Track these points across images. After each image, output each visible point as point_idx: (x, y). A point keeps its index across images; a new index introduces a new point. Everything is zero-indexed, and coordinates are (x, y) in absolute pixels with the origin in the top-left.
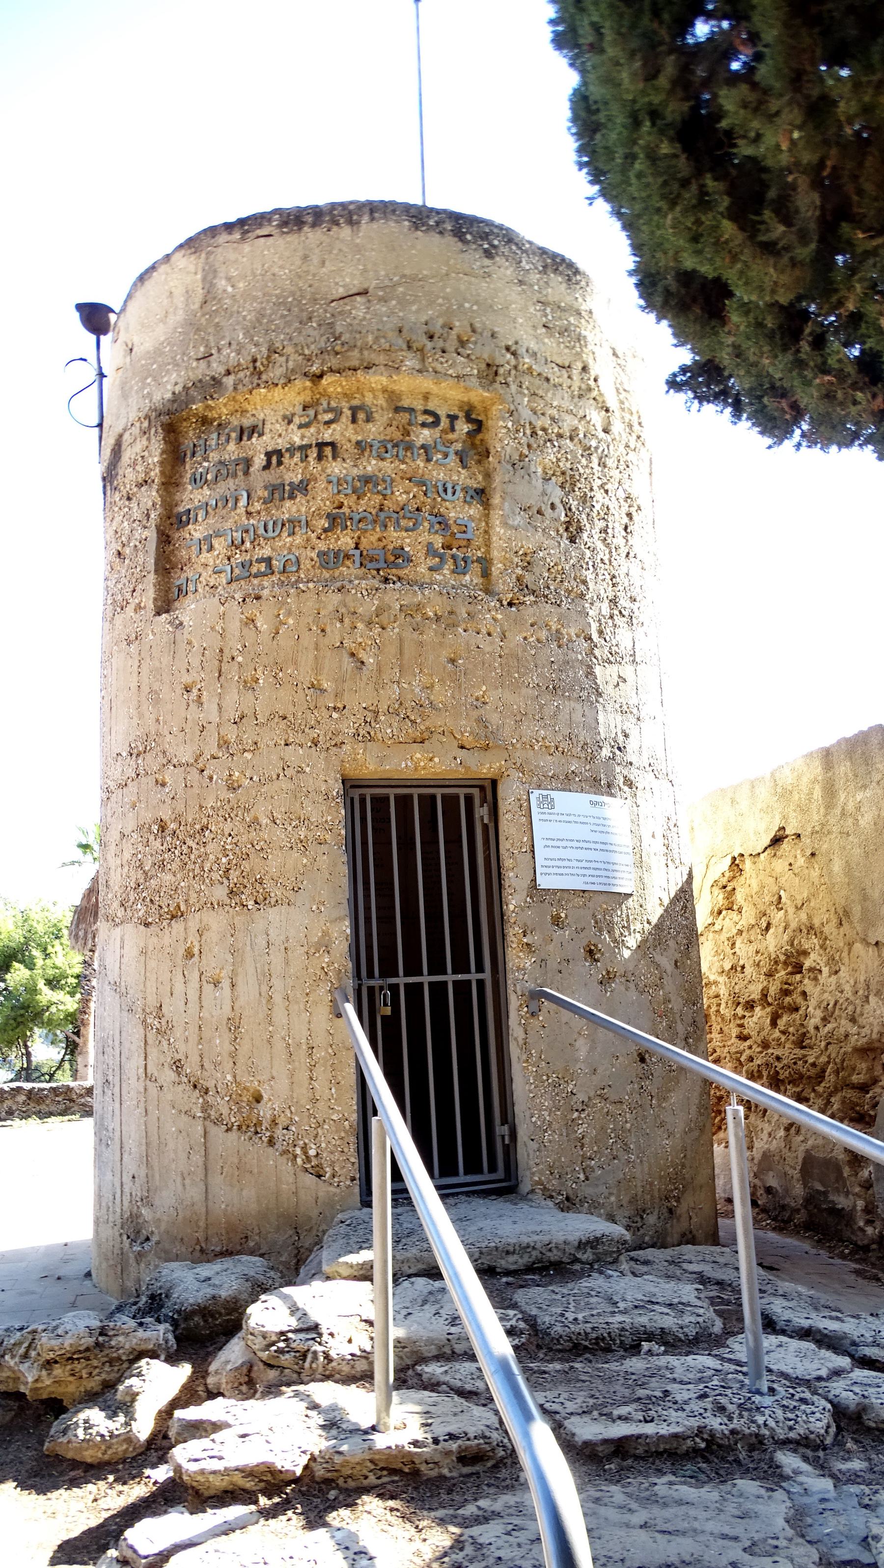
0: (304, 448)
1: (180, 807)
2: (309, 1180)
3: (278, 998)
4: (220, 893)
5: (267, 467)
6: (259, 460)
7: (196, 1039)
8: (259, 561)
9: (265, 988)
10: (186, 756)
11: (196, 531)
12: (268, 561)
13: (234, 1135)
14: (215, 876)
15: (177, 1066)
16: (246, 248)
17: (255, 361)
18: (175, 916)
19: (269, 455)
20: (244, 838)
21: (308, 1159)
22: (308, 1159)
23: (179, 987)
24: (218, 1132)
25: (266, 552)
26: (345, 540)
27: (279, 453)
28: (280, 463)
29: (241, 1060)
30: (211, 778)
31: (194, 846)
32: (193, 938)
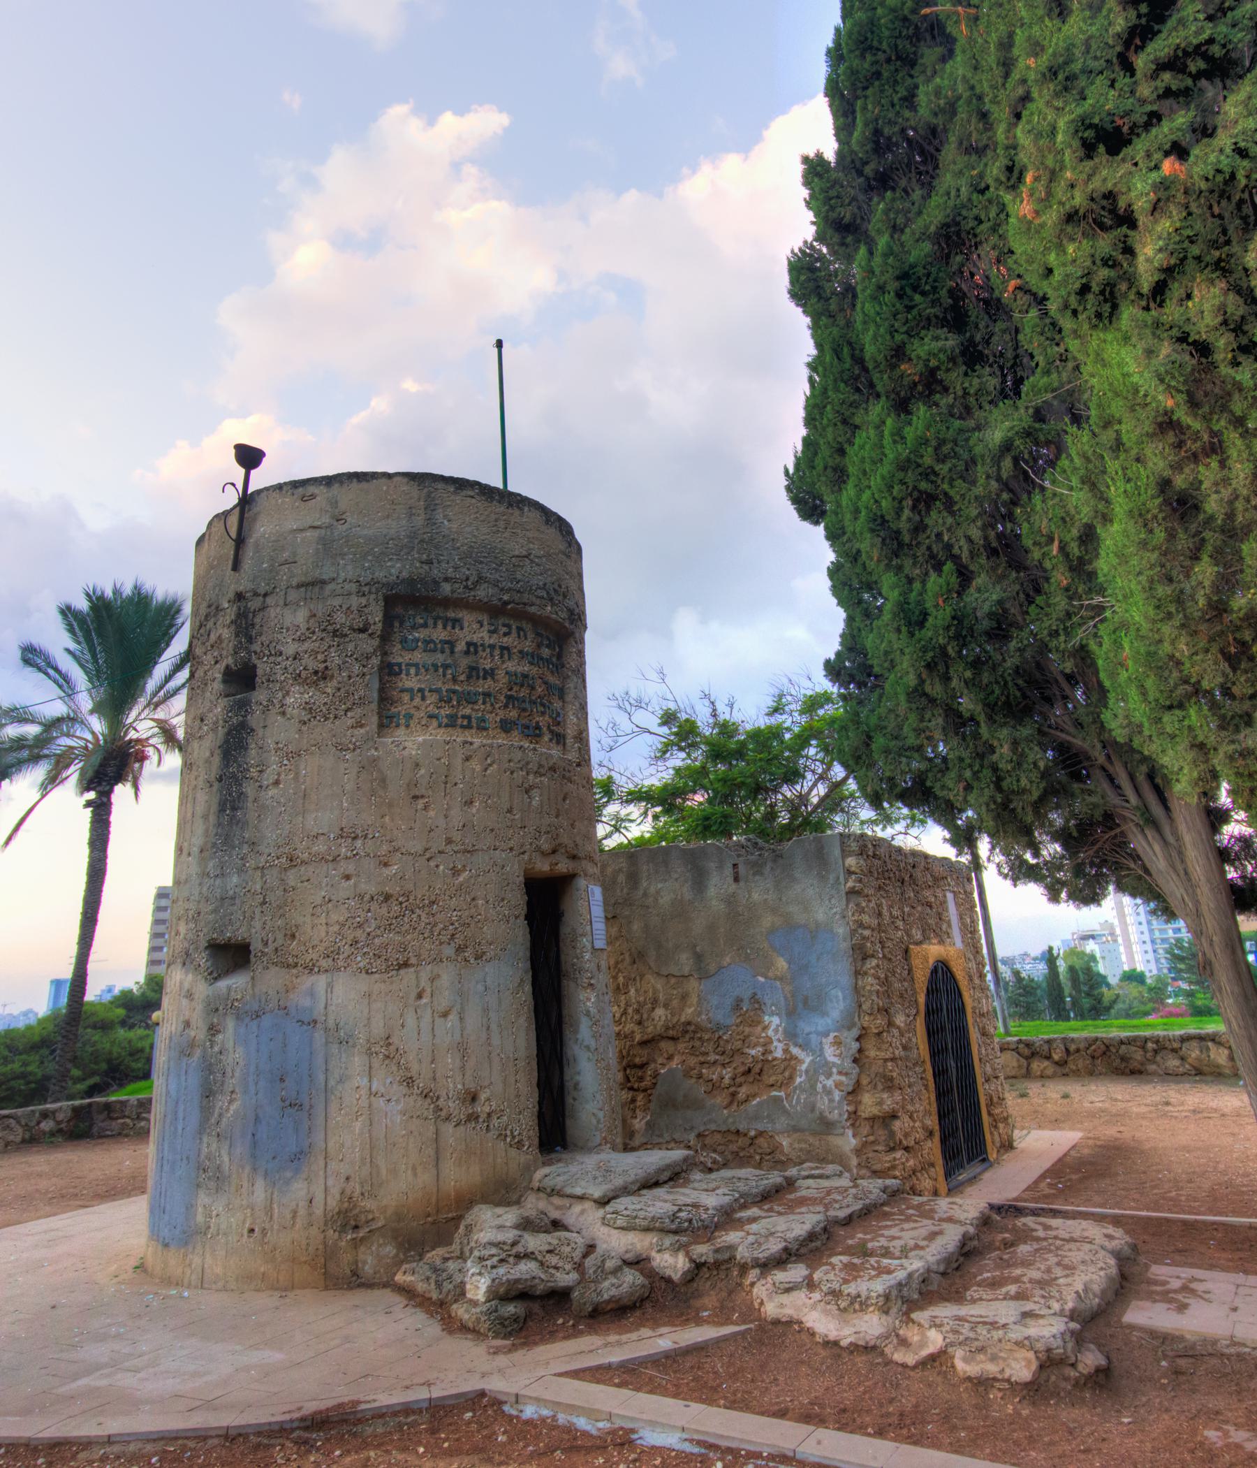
0: (492, 647)
1: (410, 886)
2: (513, 1152)
3: (494, 1026)
4: (449, 951)
5: (467, 653)
6: (460, 647)
7: (430, 1059)
8: (464, 717)
9: (485, 1020)
10: (417, 847)
11: (410, 682)
12: (469, 718)
13: (462, 1128)
14: (444, 939)
15: (409, 1081)
16: (458, 499)
17: (467, 579)
18: (406, 965)
19: (469, 644)
20: (467, 913)
21: (514, 1137)
22: (514, 1137)
23: (410, 1020)
24: (448, 1129)
25: (467, 711)
26: (513, 714)
27: (475, 645)
28: (476, 652)
29: (469, 1073)
30: (437, 866)
31: (424, 916)
32: (424, 983)
